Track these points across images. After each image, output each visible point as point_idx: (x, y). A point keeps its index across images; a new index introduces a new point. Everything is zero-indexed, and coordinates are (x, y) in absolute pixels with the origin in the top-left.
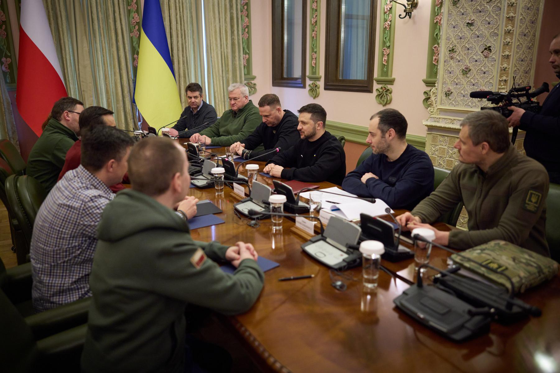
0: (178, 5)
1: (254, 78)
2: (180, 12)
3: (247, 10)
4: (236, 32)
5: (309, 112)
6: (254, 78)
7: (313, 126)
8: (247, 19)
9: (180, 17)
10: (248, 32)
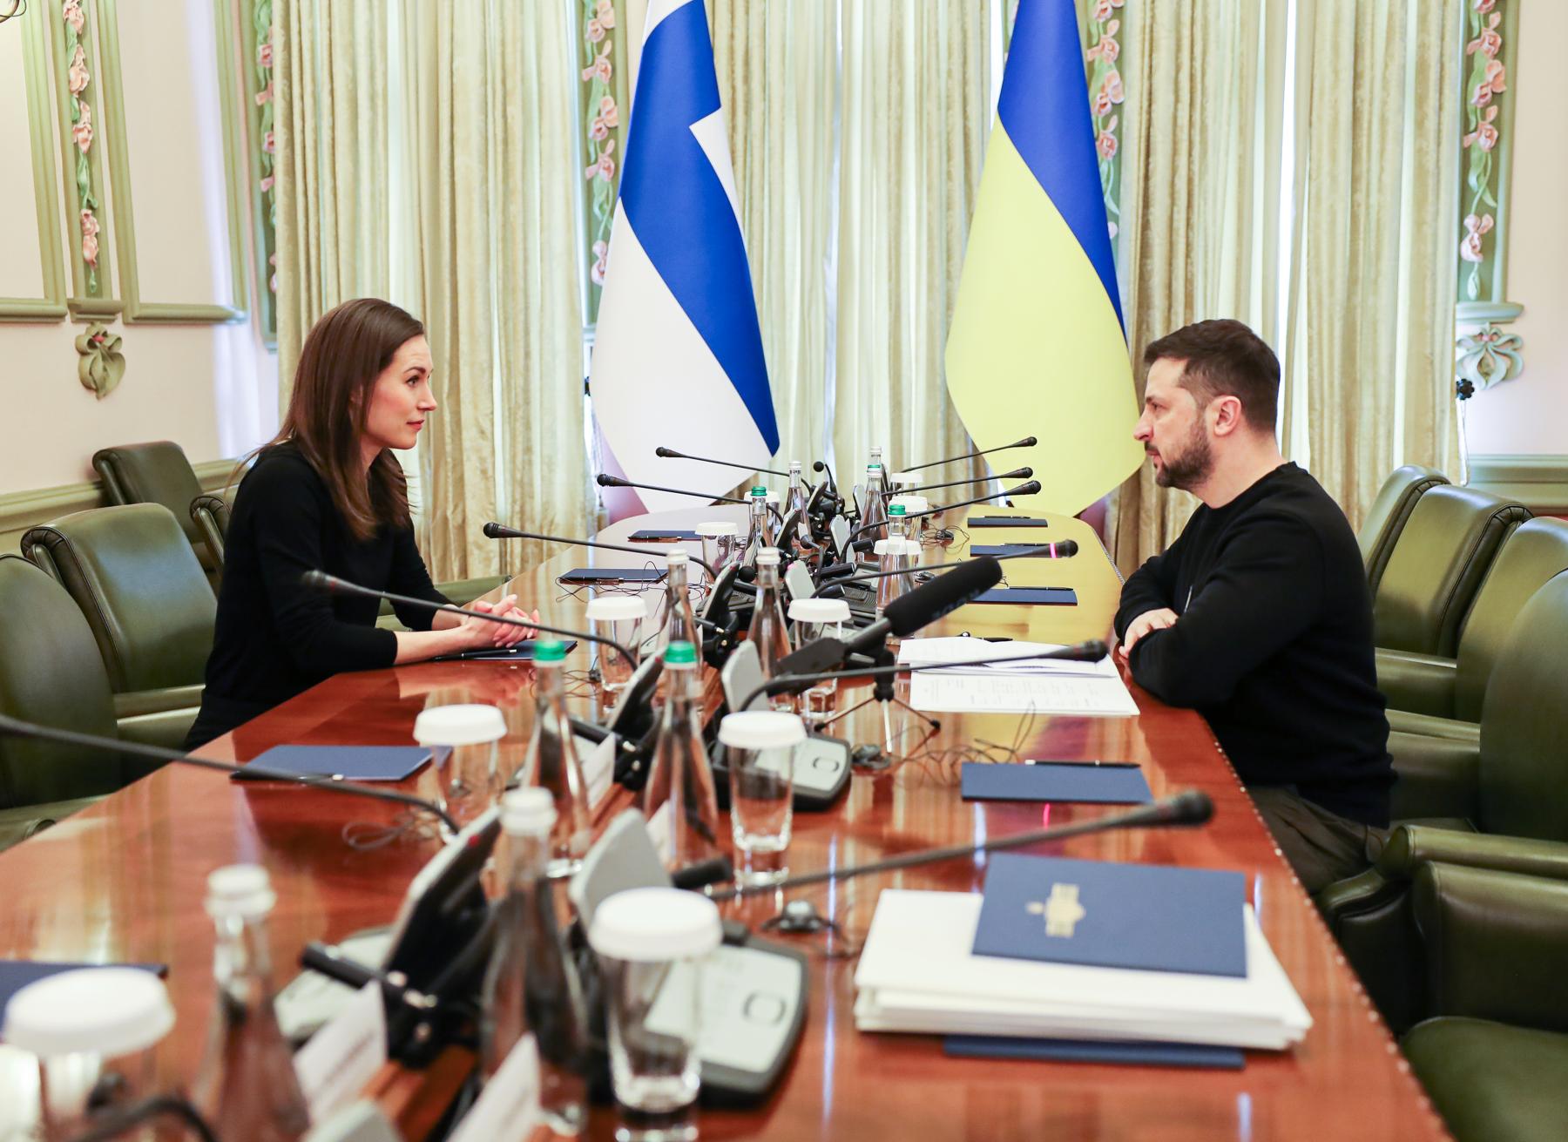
0: (1186, 33)
1: (1519, 311)
2: (1192, 59)
3: (1500, 29)
4: (1431, 124)
5: (1178, 356)
6: (1519, 311)
7: (1192, 419)
8: (1497, 67)
9: (1192, 77)
10: (1497, 123)
